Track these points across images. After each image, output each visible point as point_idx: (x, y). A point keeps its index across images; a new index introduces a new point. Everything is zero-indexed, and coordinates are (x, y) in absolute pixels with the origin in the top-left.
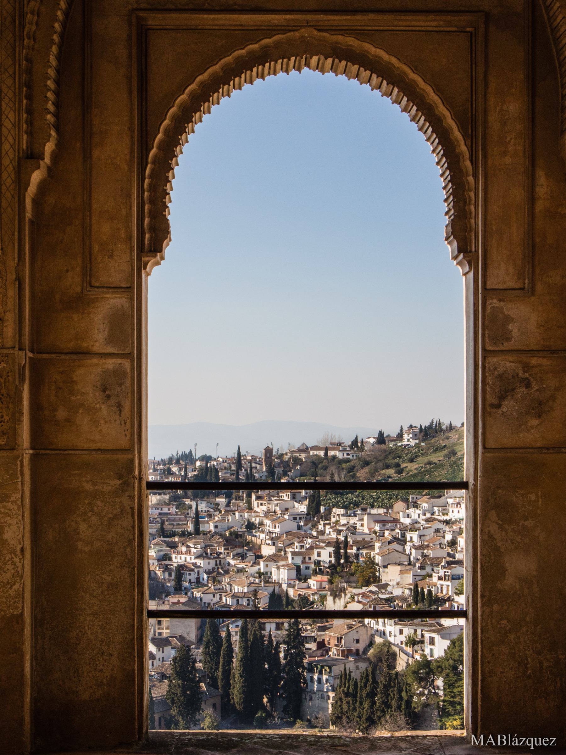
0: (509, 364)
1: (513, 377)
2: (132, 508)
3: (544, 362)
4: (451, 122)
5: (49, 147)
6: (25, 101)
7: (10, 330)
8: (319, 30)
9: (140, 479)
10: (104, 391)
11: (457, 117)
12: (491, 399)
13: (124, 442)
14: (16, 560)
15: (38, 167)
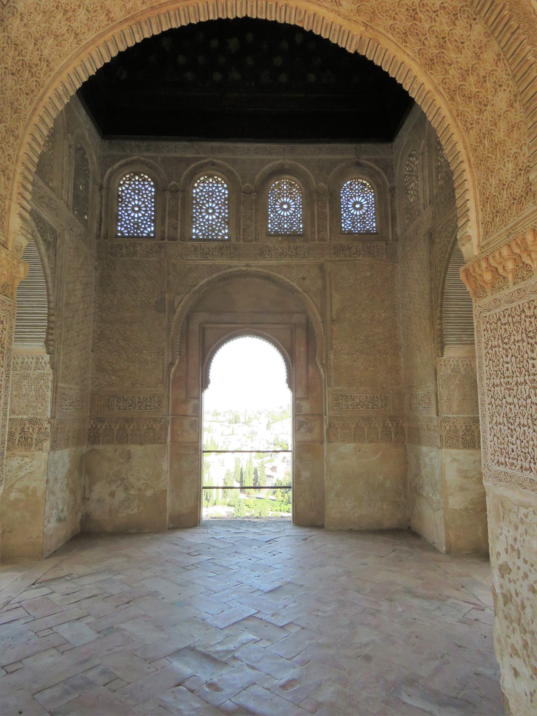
3: (312, 418)
5: (177, 362)
11: (288, 352)
12: (297, 428)
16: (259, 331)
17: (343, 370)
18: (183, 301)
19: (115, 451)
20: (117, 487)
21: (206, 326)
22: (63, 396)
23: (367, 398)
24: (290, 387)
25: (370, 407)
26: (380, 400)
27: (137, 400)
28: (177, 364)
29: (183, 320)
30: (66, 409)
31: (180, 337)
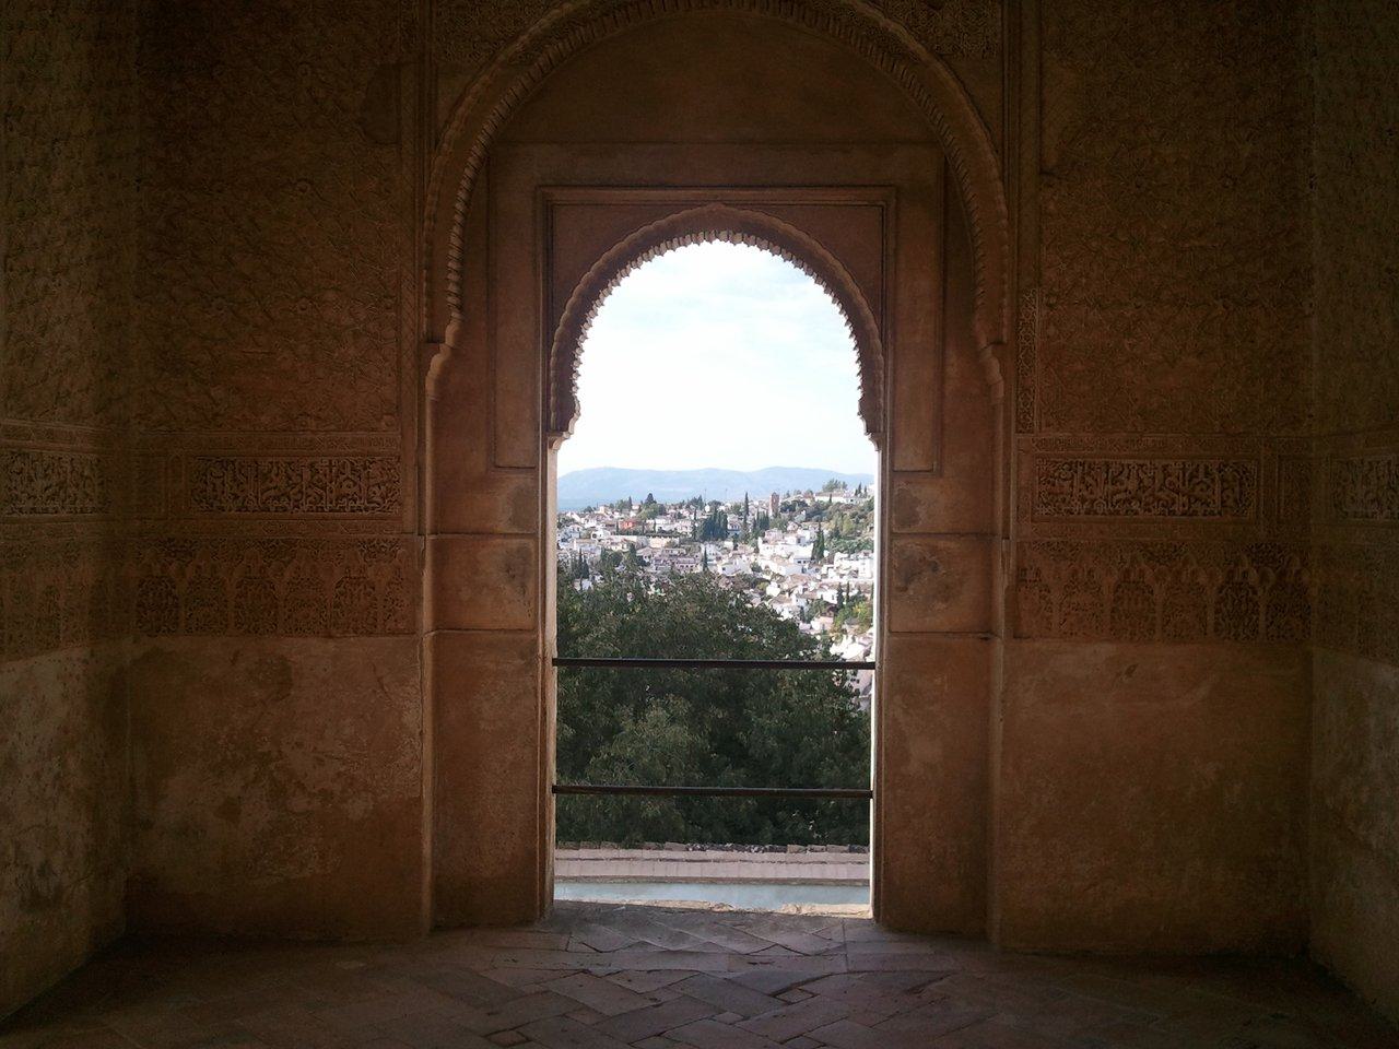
0: (915, 547)
1: (920, 561)
2: (535, 688)
3: (952, 545)
4: (860, 299)
5: (450, 332)
6: (425, 284)
7: (409, 515)
8: (726, 205)
9: (544, 659)
10: (508, 571)
12: (898, 583)
13: (527, 622)
14: (415, 744)
15: (438, 352)
16: (760, 216)
17: (1079, 367)
18: (469, 99)
19: (233, 662)
20: (244, 788)
21: (560, 196)
22: (18, 465)
23: (1167, 474)
24: (871, 429)
25: (1175, 508)
26: (1218, 490)
27: (307, 475)
28: (449, 339)
29: (468, 172)
30: (33, 510)
31: (461, 238)
